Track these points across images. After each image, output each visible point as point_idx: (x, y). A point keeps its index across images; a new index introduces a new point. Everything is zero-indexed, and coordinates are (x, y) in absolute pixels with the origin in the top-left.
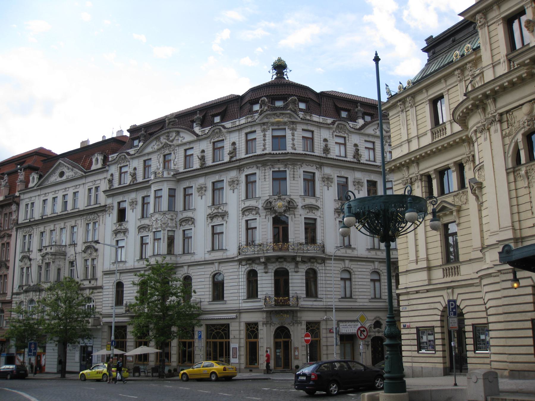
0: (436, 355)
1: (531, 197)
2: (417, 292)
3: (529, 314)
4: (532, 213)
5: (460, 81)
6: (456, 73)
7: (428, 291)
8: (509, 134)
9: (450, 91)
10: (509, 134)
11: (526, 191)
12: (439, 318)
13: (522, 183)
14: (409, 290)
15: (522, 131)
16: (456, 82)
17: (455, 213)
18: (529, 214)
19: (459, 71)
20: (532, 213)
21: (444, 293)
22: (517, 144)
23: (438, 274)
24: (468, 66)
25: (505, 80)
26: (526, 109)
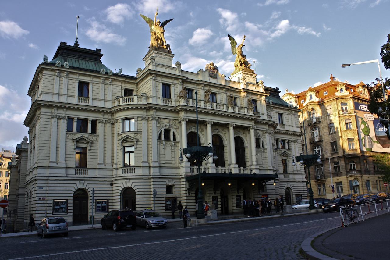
0: (67, 215)
1: (165, 153)
2: (56, 180)
3: (164, 195)
4: (165, 159)
5: (103, 83)
6: (102, 78)
7: (65, 180)
8: (159, 127)
9: (94, 84)
10: (159, 127)
11: (164, 150)
12: (72, 195)
13: (162, 147)
14: (50, 178)
15: (165, 128)
16: (100, 82)
17: (90, 144)
18: (163, 159)
19: (104, 79)
20: (165, 159)
21: (78, 182)
22: (162, 131)
23: (72, 172)
24: (110, 80)
25: (166, 108)
26: (167, 121)
